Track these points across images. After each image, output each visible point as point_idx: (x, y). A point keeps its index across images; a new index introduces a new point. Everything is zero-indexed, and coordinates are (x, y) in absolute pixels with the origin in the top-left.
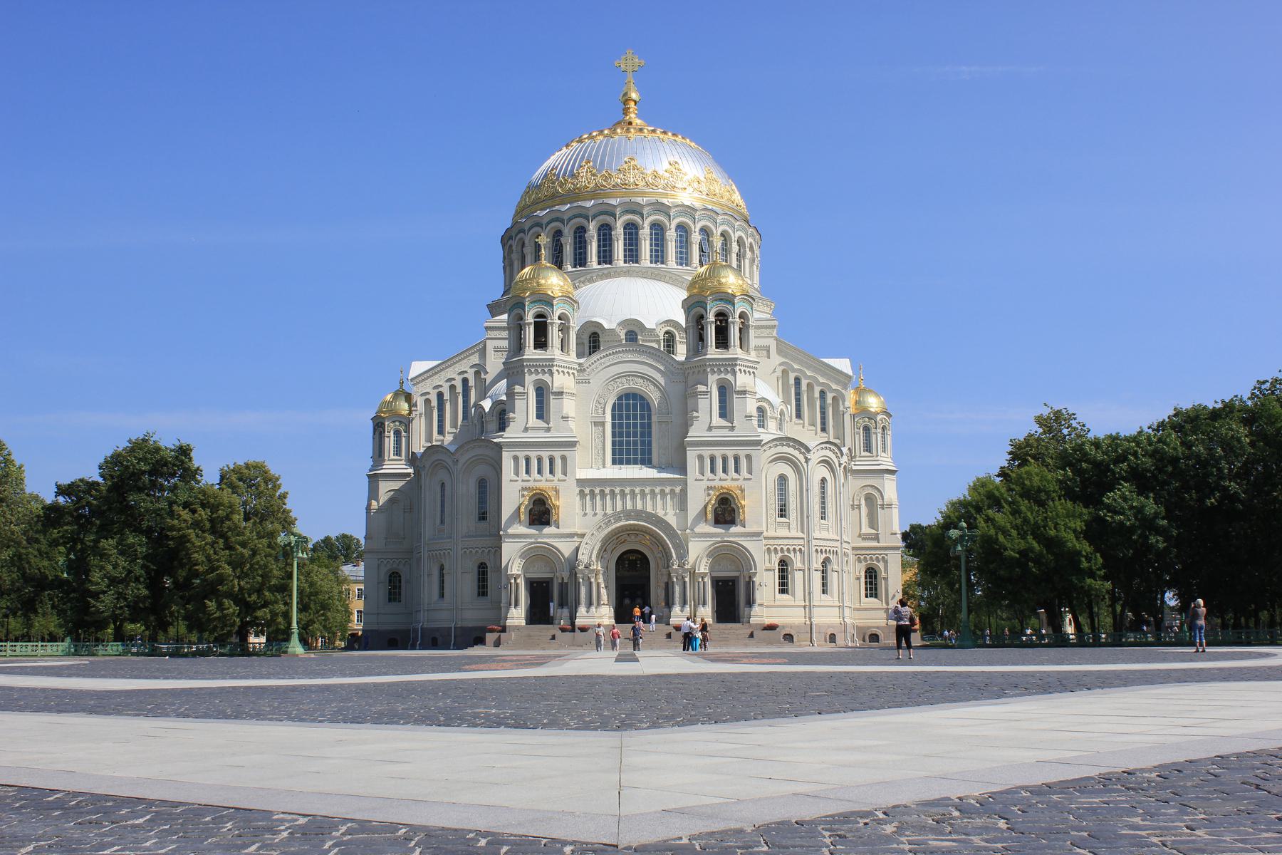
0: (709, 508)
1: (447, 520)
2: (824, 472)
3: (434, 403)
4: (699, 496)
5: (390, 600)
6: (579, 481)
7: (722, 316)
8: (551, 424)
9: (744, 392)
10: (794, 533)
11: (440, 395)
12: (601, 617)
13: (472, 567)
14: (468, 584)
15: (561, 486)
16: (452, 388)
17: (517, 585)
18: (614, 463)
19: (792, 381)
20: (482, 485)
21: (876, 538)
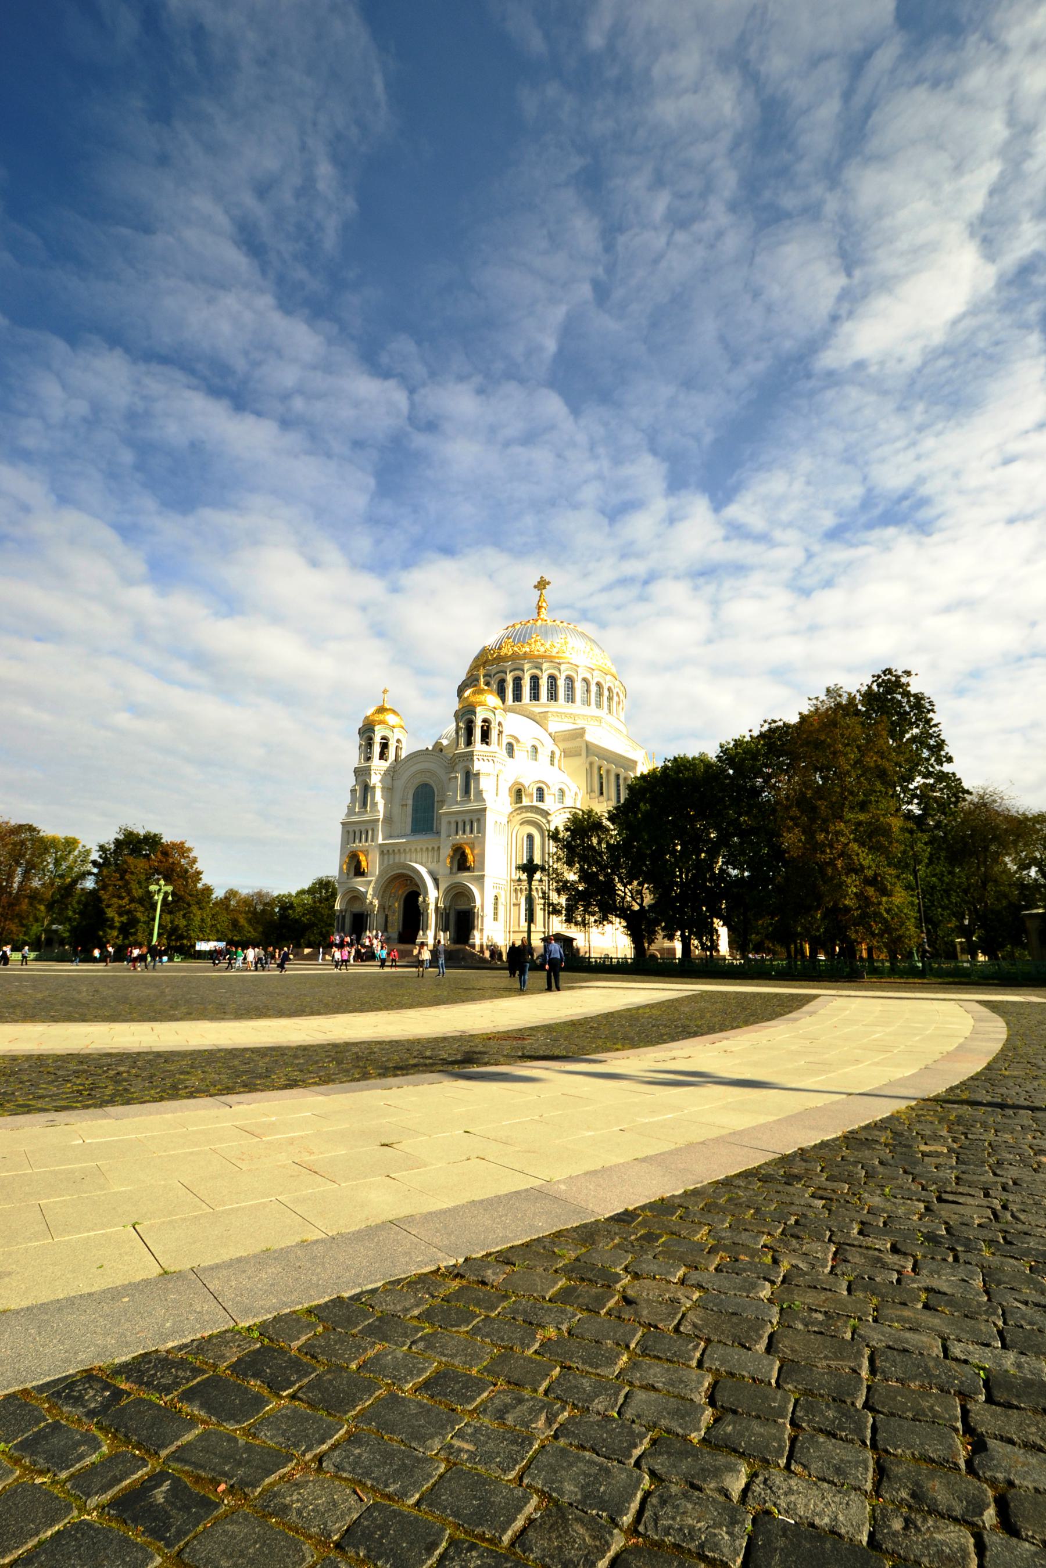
4: (446, 851)
17: (344, 917)
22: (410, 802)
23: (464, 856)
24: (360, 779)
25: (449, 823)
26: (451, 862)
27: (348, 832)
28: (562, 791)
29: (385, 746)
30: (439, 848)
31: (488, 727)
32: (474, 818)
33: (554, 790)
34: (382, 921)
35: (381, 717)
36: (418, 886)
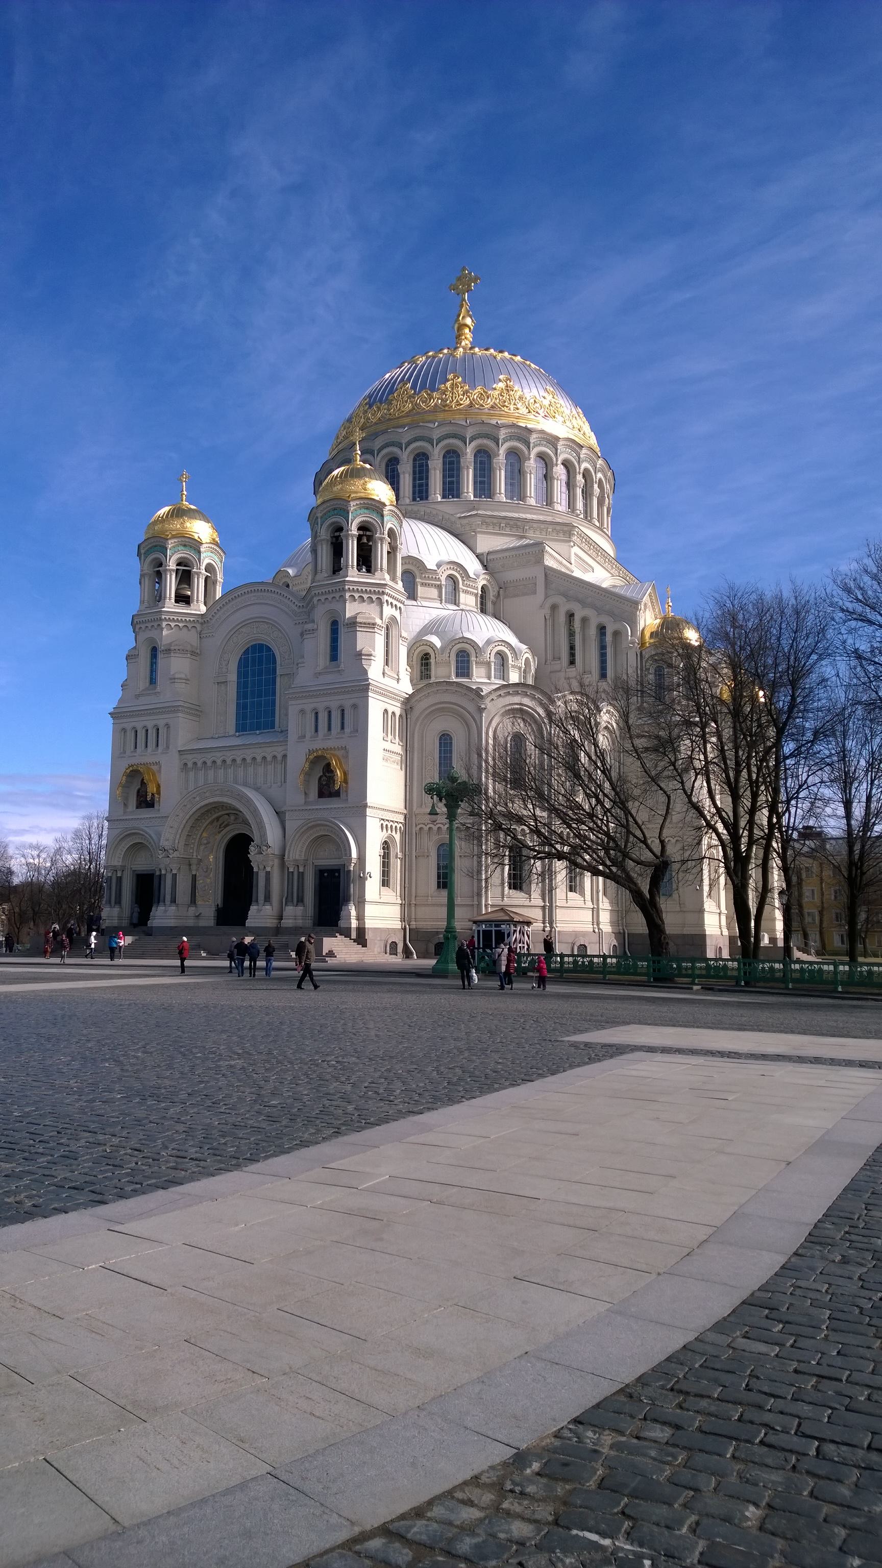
8: (158, 689)
9: (353, 624)
17: (119, 880)
19: (562, 618)
22: (233, 677)
23: (328, 769)
24: (143, 636)
25: (302, 711)
26: (307, 782)
27: (124, 730)
28: (501, 656)
29: (185, 576)
30: (285, 756)
31: (370, 538)
32: (347, 704)
33: (490, 655)
34: (183, 887)
35: (176, 525)
36: (246, 822)
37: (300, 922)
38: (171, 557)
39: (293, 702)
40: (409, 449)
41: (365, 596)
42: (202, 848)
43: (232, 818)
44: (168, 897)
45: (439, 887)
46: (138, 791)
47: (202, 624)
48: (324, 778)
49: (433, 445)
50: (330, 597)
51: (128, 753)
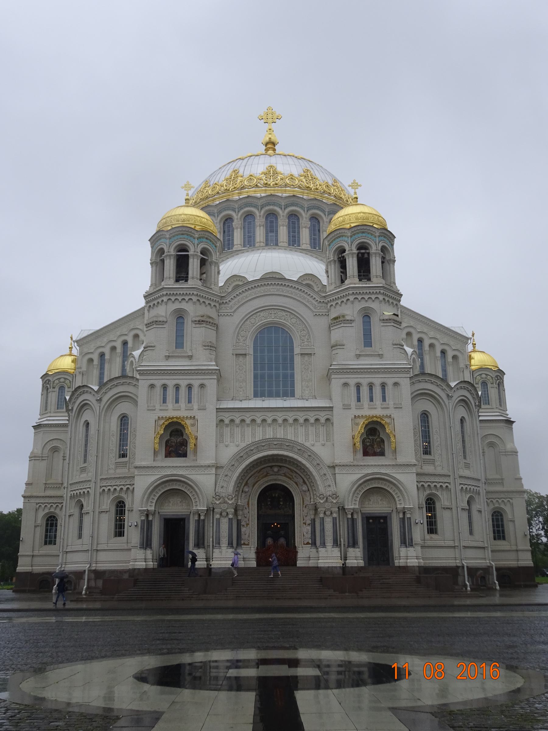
0: (358, 440)
1: (91, 458)
2: (462, 412)
3: (96, 362)
5: (46, 543)
6: (218, 410)
7: (363, 247)
10: (439, 471)
11: (102, 355)
12: (135, 560)
13: (108, 504)
14: (107, 523)
15: (199, 415)
16: (114, 348)
18: (256, 395)
20: (124, 419)
21: (501, 482)
25: (346, 385)
32: (390, 382)
37: (361, 563)
38: (198, 245)
39: (336, 376)
40: (287, 210)
41: (391, 301)
42: (243, 495)
43: (276, 469)
44: (224, 541)
45: (428, 533)
46: (167, 442)
47: (220, 304)
48: (368, 440)
49: (304, 211)
50: (366, 297)
51: (158, 407)
